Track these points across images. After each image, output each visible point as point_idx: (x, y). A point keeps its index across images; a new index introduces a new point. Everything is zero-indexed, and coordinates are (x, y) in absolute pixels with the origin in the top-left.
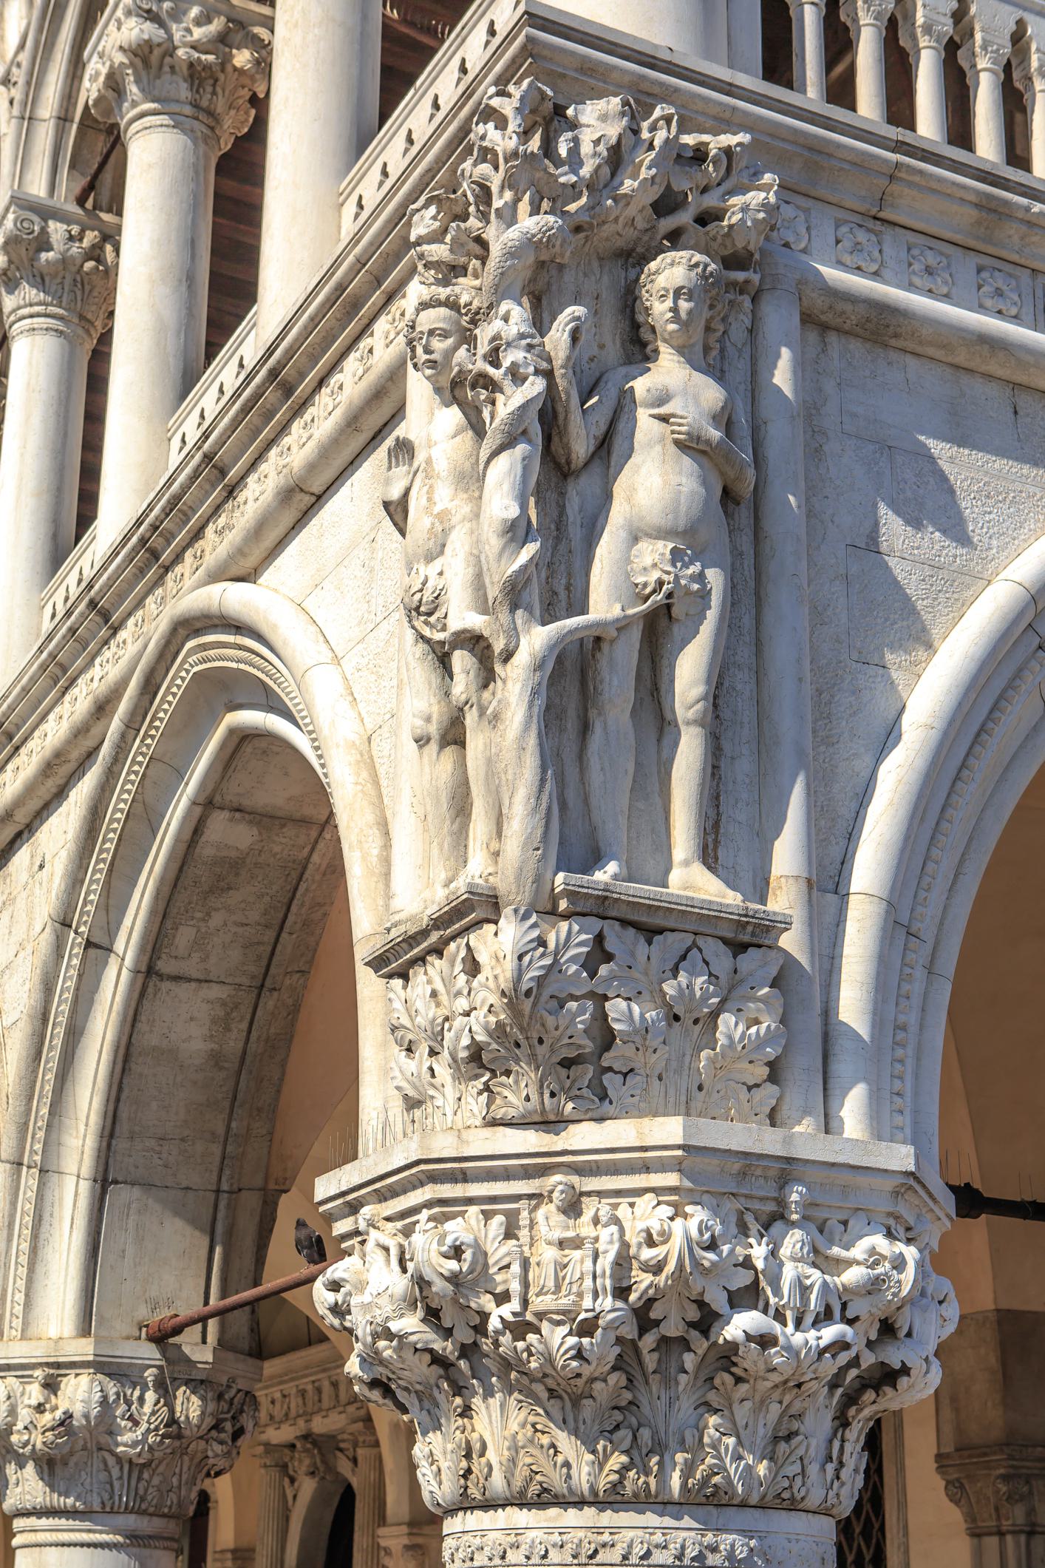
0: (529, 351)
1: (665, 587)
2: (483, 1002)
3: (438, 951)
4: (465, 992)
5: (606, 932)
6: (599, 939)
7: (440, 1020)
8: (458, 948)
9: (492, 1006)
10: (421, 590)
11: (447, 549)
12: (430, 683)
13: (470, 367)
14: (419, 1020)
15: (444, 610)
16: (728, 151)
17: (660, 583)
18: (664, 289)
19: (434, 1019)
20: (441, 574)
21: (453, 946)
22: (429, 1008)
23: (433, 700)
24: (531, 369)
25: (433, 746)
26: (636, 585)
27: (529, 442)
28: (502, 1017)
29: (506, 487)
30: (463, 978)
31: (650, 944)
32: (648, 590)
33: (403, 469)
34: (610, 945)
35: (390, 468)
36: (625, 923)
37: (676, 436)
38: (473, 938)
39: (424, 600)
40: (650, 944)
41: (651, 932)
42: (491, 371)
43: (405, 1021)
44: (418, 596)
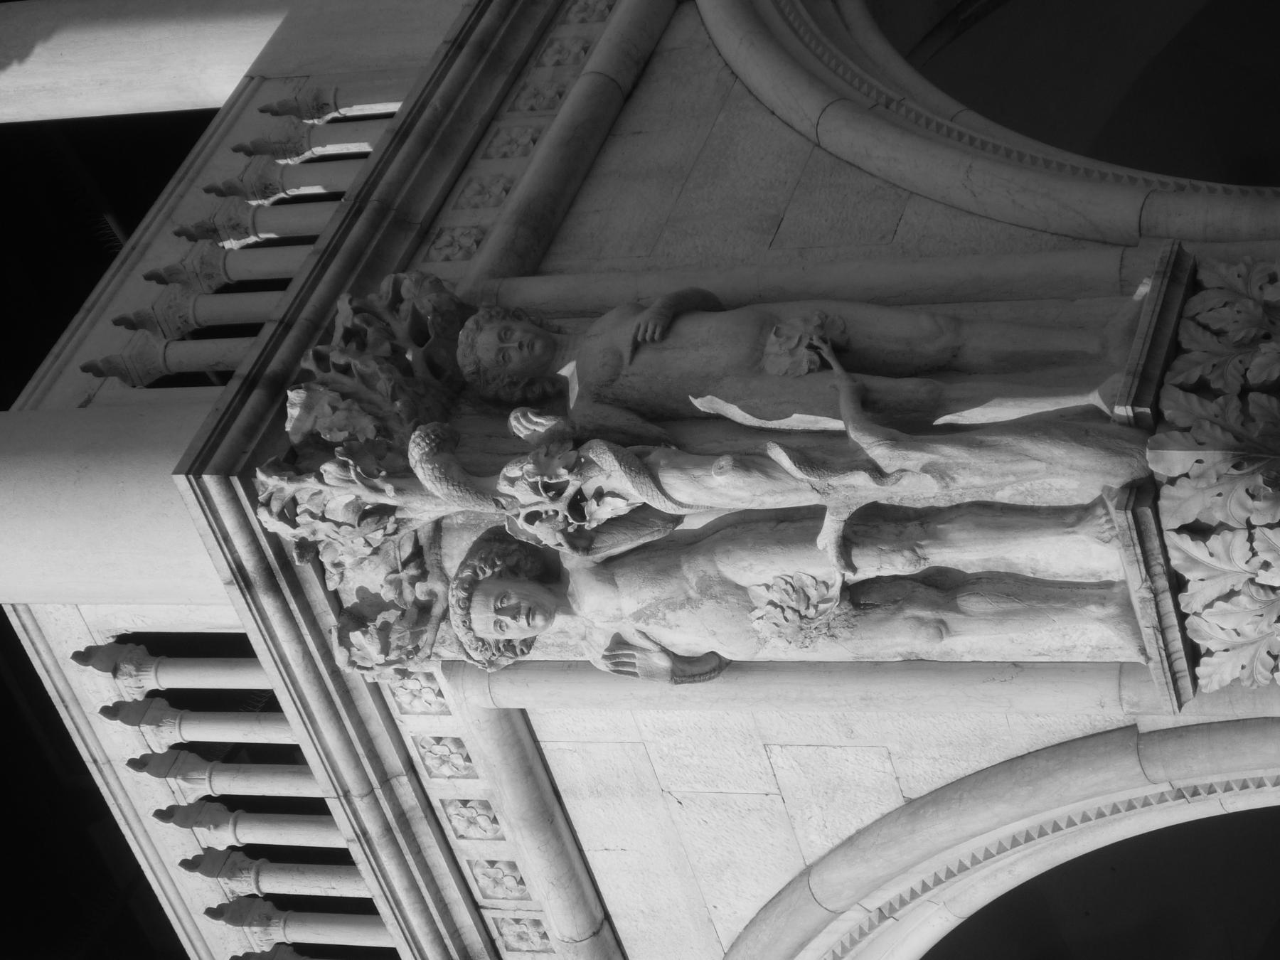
0: (553, 457)
1: (816, 342)
2: (1243, 506)
3: (1178, 584)
4: (1227, 535)
5: (1180, 379)
6: (1184, 388)
7: (1253, 589)
8: (1178, 549)
9: (1247, 491)
10: (782, 608)
11: (742, 583)
12: (880, 621)
13: (560, 517)
14: (1248, 629)
15: (809, 581)
16: (356, 311)
17: (811, 347)
18: (497, 355)
19: (1252, 597)
20: (768, 587)
21: (1176, 561)
22: (1238, 605)
23: (901, 616)
24: (573, 454)
25: (948, 617)
26: (810, 371)
27: (649, 453)
28: (1260, 480)
29: (698, 473)
30: (1215, 542)
31: (1187, 351)
32: (816, 358)
33: (639, 659)
34: (1194, 376)
35: (635, 674)
36: (1167, 367)
37: (657, 336)
38: (1170, 522)
39: (793, 604)
40: (1187, 351)
41: (1177, 350)
42: (570, 491)
43: (1244, 657)
44: (789, 614)
